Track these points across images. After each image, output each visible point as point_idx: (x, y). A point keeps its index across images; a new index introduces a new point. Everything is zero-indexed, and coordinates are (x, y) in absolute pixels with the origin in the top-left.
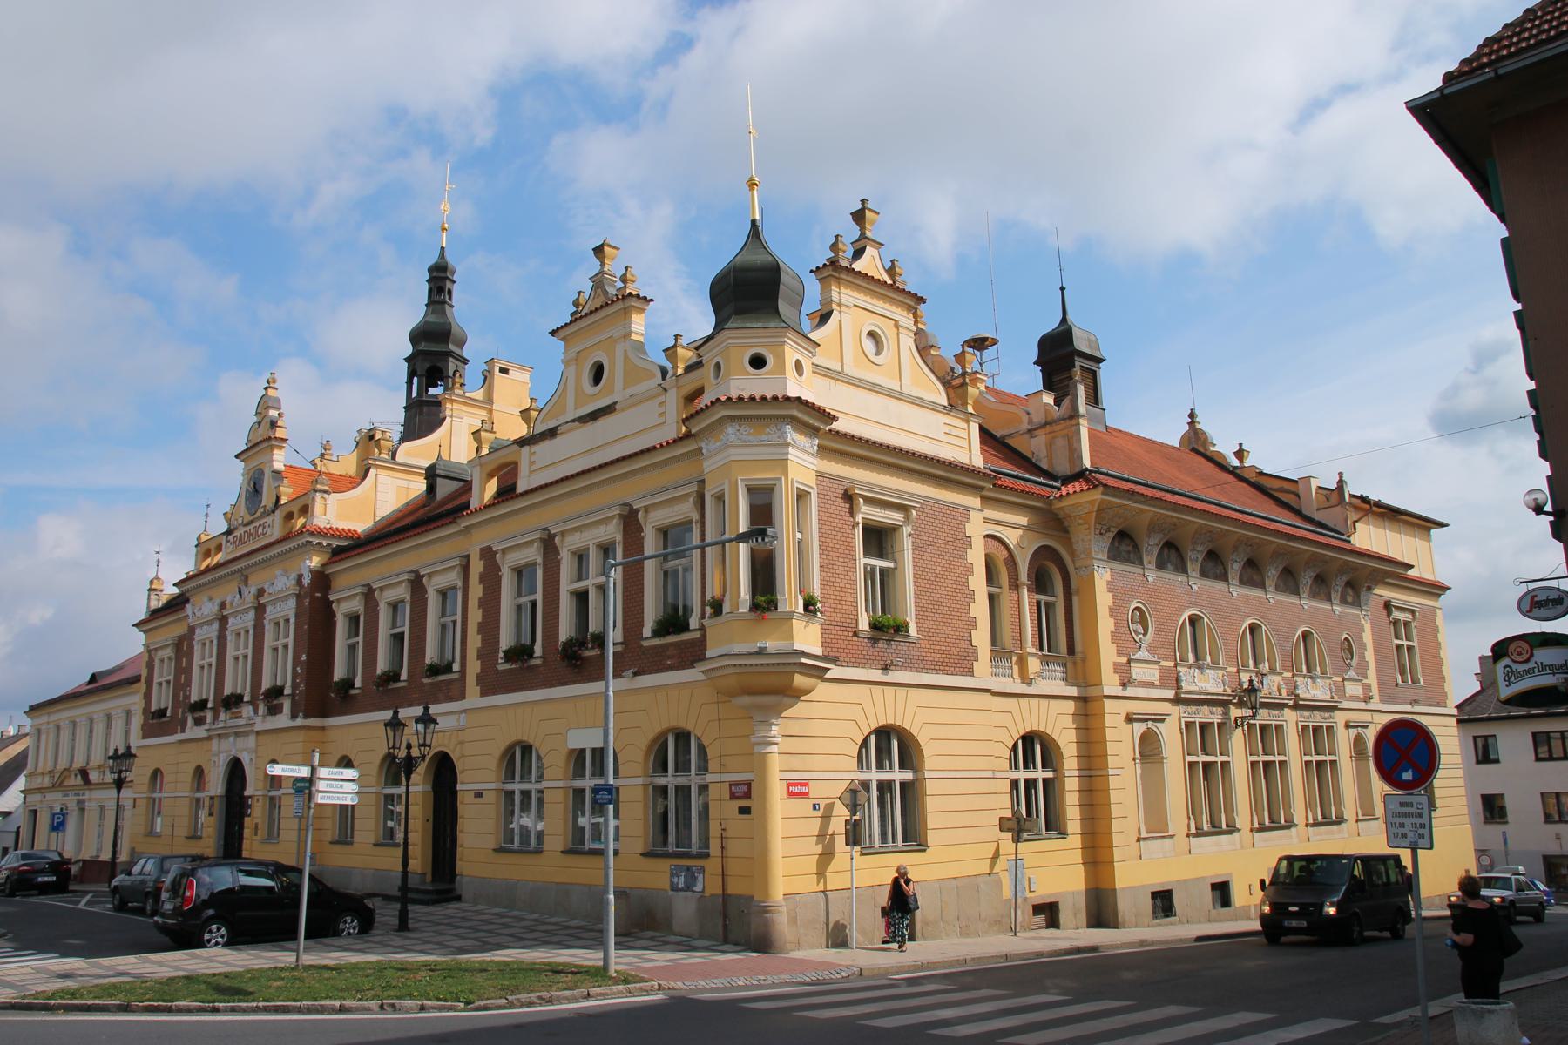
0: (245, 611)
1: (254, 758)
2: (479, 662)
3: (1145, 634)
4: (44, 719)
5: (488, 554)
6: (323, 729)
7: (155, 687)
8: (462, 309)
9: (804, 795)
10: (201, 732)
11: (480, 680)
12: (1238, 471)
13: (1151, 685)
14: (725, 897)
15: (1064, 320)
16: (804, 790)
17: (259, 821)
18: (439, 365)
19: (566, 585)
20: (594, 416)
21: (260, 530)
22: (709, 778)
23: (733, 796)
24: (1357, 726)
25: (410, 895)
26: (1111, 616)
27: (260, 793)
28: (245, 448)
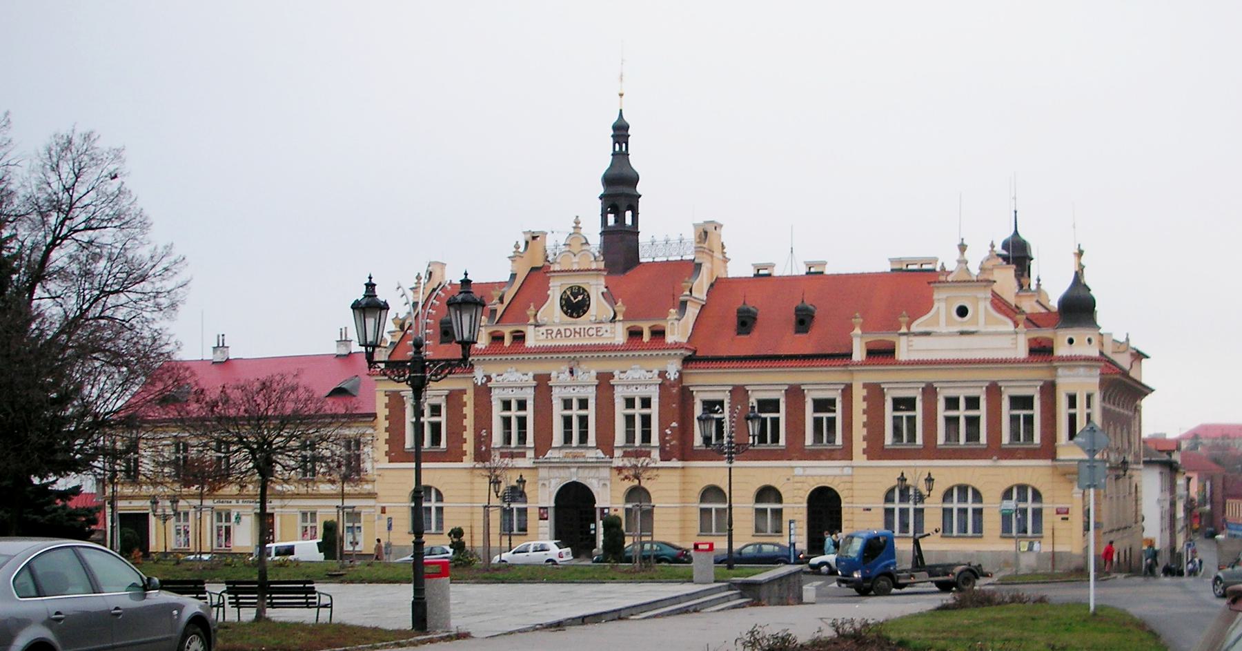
1: (608, 483)
8: (637, 160)
11: (865, 451)
14: (1053, 553)
19: (942, 412)
20: (962, 333)
21: (591, 332)
23: (1058, 513)
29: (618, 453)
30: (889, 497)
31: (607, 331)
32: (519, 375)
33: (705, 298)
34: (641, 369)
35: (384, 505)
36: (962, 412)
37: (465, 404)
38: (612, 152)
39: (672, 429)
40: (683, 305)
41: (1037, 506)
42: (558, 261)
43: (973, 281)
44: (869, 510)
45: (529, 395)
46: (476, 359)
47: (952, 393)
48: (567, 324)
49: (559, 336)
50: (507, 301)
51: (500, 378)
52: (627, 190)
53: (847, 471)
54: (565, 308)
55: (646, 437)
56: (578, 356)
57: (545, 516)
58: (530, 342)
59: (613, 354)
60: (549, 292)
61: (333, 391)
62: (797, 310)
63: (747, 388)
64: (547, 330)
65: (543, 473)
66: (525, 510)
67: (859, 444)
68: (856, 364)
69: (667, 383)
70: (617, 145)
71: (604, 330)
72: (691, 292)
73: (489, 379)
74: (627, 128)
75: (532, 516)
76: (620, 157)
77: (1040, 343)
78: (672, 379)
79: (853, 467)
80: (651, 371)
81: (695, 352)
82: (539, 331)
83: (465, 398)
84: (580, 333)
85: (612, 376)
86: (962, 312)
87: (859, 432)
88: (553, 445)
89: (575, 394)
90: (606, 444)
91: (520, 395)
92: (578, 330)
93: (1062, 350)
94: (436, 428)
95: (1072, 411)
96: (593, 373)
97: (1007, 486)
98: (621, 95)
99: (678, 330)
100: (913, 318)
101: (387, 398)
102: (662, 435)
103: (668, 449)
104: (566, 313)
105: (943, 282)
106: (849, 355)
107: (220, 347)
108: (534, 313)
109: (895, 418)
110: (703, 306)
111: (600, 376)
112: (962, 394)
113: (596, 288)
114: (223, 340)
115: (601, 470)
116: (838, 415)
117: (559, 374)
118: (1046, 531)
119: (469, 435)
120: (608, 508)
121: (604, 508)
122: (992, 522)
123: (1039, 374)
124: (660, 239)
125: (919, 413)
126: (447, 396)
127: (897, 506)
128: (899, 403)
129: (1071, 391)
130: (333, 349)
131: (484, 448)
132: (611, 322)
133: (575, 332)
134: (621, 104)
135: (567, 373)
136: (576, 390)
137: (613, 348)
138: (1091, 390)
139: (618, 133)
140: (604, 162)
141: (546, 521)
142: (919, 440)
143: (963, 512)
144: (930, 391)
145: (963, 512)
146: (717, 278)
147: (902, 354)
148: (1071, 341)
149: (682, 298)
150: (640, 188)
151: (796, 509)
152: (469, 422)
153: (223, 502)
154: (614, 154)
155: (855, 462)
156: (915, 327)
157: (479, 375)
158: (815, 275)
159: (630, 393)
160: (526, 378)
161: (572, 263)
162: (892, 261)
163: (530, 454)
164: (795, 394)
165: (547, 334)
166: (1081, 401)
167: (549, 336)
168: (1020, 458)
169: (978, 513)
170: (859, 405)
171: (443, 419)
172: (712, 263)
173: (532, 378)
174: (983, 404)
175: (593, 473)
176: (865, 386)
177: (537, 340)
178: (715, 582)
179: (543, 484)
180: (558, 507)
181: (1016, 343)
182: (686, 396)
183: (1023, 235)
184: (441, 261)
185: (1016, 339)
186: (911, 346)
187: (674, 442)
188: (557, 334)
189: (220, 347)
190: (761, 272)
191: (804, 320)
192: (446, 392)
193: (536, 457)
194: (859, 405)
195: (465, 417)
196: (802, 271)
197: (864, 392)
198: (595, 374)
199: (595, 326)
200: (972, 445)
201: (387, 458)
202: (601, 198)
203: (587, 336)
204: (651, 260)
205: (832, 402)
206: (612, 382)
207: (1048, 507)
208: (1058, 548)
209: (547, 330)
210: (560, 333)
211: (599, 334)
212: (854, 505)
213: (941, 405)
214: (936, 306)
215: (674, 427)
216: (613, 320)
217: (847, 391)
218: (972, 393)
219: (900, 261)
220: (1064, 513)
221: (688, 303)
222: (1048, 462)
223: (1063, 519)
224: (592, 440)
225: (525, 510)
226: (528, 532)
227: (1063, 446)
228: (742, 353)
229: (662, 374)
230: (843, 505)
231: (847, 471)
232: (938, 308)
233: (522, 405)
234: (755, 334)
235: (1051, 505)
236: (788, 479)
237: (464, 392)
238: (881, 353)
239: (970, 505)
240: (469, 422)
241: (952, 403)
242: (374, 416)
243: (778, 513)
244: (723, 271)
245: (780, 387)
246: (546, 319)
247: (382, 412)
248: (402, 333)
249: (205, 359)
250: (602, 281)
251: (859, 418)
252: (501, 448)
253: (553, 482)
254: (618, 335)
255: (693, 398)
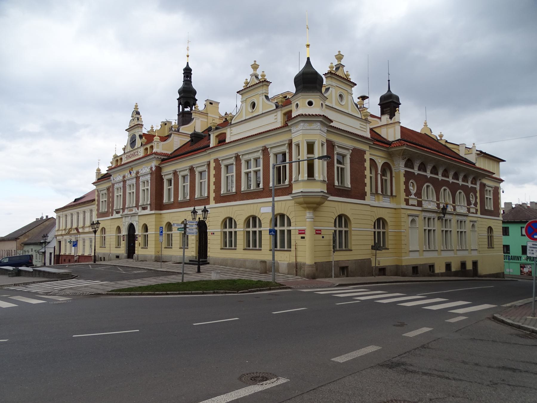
0: (133, 178)
1: (138, 223)
2: (214, 193)
3: (413, 190)
4: (61, 213)
5: (216, 161)
6: (161, 214)
7: (101, 202)
8: (195, 85)
9: (320, 234)
10: (118, 216)
11: (215, 199)
12: (439, 141)
13: (414, 205)
14: (296, 264)
15: (389, 90)
16: (320, 232)
17: (140, 242)
19: (244, 170)
21: (136, 153)
22: (291, 228)
24: (473, 222)
25: (197, 263)
26: (404, 184)
27: (141, 234)
28: (128, 128)
47: (247, 157)
74: (191, 70)
98: (188, 56)
118: (293, 248)
134: (188, 60)
138: (311, 139)
183: (394, 92)
218: (256, 155)
229: (151, 168)
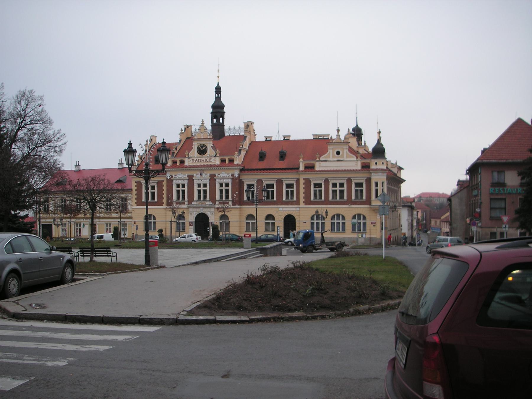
1: (214, 213)
8: (223, 100)
11: (304, 202)
14: (370, 238)
18: (217, 115)
20: (338, 161)
21: (208, 160)
23: (372, 224)
29: (217, 203)
30: (312, 218)
31: (213, 160)
32: (182, 175)
33: (248, 148)
34: (225, 173)
35: (135, 221)
36: (338, 188)
37: (163, 186)
38: (215, 97)
39: (236, 194)
40: (240, 151)
41: (364, 221)
42: (196, 135)
43: (342, 142)
44: (305, 223)
45: (186, 182)
46: (167, 170)
47: (335, 182)
48: (199, 157)
49: (196, 162)
50: (178, 149)
51: (176, 177)
52: (220, 110)
53: (298, 209)
54: (198, 152)
55: (227, 197)
56: (203, 169)
57: (192, 225)
58: (186, 164)
59: (215, 168)
60: (193, 146)
61: (117, 181)
62: (280, 152)
63: (263, 180)
64: (192, 160)
65: (191, 210)
66: (185, 223)
67: (302, 200)
68: (301, 172)
69: (235, 178)
70: (217, 95)
71: (212, 159)
72: (243, 146)
73: (172, 177)
74: (220, 88)
75: (187, 225)
76: (218, 98)
77: (366, 164)
78: (236, 177)
79: (300, 208)
80: (229, 174)
81: (244, 167)
82: (189, 160)
83: (163, 183)
84: (204, 161)
85: (215, 176)
86: (338, 153)
87: (302, 195)
88: (194, 200)
89: (202, 182)
90: (213, 199)
91: (183, 182)
92: (203, 160)
93: (373, 167)
94: (153, 194)
95: (377, 188)
96: (208, 175)
97: (354, 214)
98: (218, 77)
99: (238, 160)
100: (321, 156)
101: (136, 183)
102: (233, 196)
103: (235, 201)
104: (199, 154)
105: (331, 143)
106: (299, 168)
107: (77, 165)
108: (187, 153)
109: (314, 190)
110: (247, 151)
111: (211, 176)
112: (338, 182)
113: (209, 145)
114: (78, 163)
115: (211, 209)
116: (295, 189)
117: (196, 175)
118: (368, 230)
119: (165, 196)
120: (214, 222)
121: (212, 222)
122: (349, 227)
123: (365, 175)
124: (232, 127)
125: (323, 189)
126: (157, 183)
127: (315, 221)
128: (316, 185)
129: (376, 181)
130: (117, 166)
131: (170, 201)
132: (215, 157)
133: (202, 160)
134: (218, 80)
135: (199, 175)
136: (202, 181)
137: (215, 166)
138: (383, 181)
139: (217, 90)
140: (213, 100)
141: (192, 227)
142: (323, 198)
143: (338, 223)
144: (327, 181)
145: (338, 223)
146: (252, 141)
147: (317, 168)
148: (376, 163)
149: (240, 148)
150: (225, 110)
151: (280, 222)
152: (165, 192)
153: (78, 220)
154: (216, 98)
155: (300, 206)
156: (321, 159)
157: (168, 175)
158: (286, 140)
159: (221, 181)
160: (185, 176)
161: (201, 136)
162: (313, 135)
163: (186, 203)
164: (279, 182)
165: (192, 161)
166: (380, 185)
167: (193, 162)
168: (358, 205)
169: (344, 224)
170: (302, 186)
171: (156, 191)
172: (250, 136)
173: (187, 176)
174: (345, 185)
175: (208, 210)
176: (304, 179)
177: (189, 163)
178: (251, 248)
179: (191, 214)
180: (196, 222)
181: (357, 164)
182: (241, 183)
183: (360, 126)
184: (155, 135)
185: (357, 163)
186: (320, 165)
187: (237, 199)
188: (196, 161)
189: (77, 165)
190: (267, 139)
191: (282, 156)
192: (157, 181)
193: (188, 204)
194: (302, 186)
195: (163, 190)
196: (282, 139)
197: (304, 181)
198: (209, 175)
199: (209, 158)
200: (342, 200)
201: (136, 204)
202: (211, 113)
203: (206, 162)
204: (229, 135)
205: (292, 185)
206: (215, 178)
207: (368, 222)
208: (372, 236)
209: (192, 160)
210: (197, 160)
211: (211, 161)
212: (300, 221)
213: (331, 186)
214: (329, 151)
215: (237, 194)
216: (216, 156)
217: (298, 181)
218: (342, 181)
219: (316, 135)
220: (374, 224)
221: (242, 150)
222: (368, 206)
223: (373, 226)
224: (208, 198)
225: (185, 223)
226: (186, 231)
227: (374, 200)
228: (261, 168)
229: (233, 175)
230: (296, 221)
231: (298, 209)
232: (330, 152)
233: (183, 186)
234: (265, 161)
235: (369, 221)
236: (277, 212)
237: (163, 181)
238: (310, 168)
239: (341, 221)
240: (165, 192)
241: (335, 185)
242: (132, 190)
243: (273, 224)
244: (254, 139)
245: (274, 180)
246: (192, 156)
247: (134, 188)
248: (141, 161)
249: (72, 170)
250: (212, 142)
251: (302, 191)
252: (176, 201)
253: (194, 213)
254: (217, 161)
255: (243, 183)
